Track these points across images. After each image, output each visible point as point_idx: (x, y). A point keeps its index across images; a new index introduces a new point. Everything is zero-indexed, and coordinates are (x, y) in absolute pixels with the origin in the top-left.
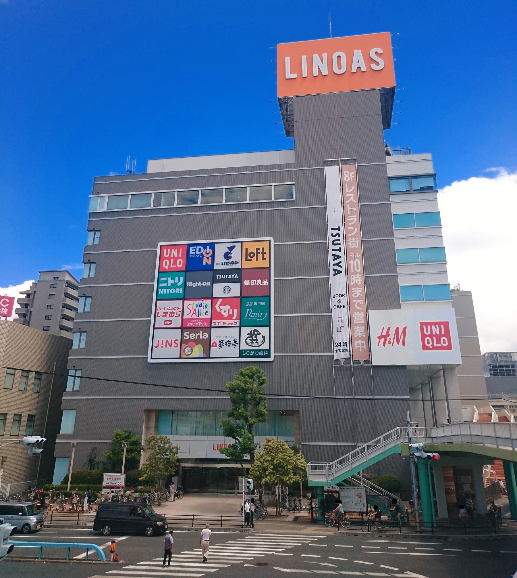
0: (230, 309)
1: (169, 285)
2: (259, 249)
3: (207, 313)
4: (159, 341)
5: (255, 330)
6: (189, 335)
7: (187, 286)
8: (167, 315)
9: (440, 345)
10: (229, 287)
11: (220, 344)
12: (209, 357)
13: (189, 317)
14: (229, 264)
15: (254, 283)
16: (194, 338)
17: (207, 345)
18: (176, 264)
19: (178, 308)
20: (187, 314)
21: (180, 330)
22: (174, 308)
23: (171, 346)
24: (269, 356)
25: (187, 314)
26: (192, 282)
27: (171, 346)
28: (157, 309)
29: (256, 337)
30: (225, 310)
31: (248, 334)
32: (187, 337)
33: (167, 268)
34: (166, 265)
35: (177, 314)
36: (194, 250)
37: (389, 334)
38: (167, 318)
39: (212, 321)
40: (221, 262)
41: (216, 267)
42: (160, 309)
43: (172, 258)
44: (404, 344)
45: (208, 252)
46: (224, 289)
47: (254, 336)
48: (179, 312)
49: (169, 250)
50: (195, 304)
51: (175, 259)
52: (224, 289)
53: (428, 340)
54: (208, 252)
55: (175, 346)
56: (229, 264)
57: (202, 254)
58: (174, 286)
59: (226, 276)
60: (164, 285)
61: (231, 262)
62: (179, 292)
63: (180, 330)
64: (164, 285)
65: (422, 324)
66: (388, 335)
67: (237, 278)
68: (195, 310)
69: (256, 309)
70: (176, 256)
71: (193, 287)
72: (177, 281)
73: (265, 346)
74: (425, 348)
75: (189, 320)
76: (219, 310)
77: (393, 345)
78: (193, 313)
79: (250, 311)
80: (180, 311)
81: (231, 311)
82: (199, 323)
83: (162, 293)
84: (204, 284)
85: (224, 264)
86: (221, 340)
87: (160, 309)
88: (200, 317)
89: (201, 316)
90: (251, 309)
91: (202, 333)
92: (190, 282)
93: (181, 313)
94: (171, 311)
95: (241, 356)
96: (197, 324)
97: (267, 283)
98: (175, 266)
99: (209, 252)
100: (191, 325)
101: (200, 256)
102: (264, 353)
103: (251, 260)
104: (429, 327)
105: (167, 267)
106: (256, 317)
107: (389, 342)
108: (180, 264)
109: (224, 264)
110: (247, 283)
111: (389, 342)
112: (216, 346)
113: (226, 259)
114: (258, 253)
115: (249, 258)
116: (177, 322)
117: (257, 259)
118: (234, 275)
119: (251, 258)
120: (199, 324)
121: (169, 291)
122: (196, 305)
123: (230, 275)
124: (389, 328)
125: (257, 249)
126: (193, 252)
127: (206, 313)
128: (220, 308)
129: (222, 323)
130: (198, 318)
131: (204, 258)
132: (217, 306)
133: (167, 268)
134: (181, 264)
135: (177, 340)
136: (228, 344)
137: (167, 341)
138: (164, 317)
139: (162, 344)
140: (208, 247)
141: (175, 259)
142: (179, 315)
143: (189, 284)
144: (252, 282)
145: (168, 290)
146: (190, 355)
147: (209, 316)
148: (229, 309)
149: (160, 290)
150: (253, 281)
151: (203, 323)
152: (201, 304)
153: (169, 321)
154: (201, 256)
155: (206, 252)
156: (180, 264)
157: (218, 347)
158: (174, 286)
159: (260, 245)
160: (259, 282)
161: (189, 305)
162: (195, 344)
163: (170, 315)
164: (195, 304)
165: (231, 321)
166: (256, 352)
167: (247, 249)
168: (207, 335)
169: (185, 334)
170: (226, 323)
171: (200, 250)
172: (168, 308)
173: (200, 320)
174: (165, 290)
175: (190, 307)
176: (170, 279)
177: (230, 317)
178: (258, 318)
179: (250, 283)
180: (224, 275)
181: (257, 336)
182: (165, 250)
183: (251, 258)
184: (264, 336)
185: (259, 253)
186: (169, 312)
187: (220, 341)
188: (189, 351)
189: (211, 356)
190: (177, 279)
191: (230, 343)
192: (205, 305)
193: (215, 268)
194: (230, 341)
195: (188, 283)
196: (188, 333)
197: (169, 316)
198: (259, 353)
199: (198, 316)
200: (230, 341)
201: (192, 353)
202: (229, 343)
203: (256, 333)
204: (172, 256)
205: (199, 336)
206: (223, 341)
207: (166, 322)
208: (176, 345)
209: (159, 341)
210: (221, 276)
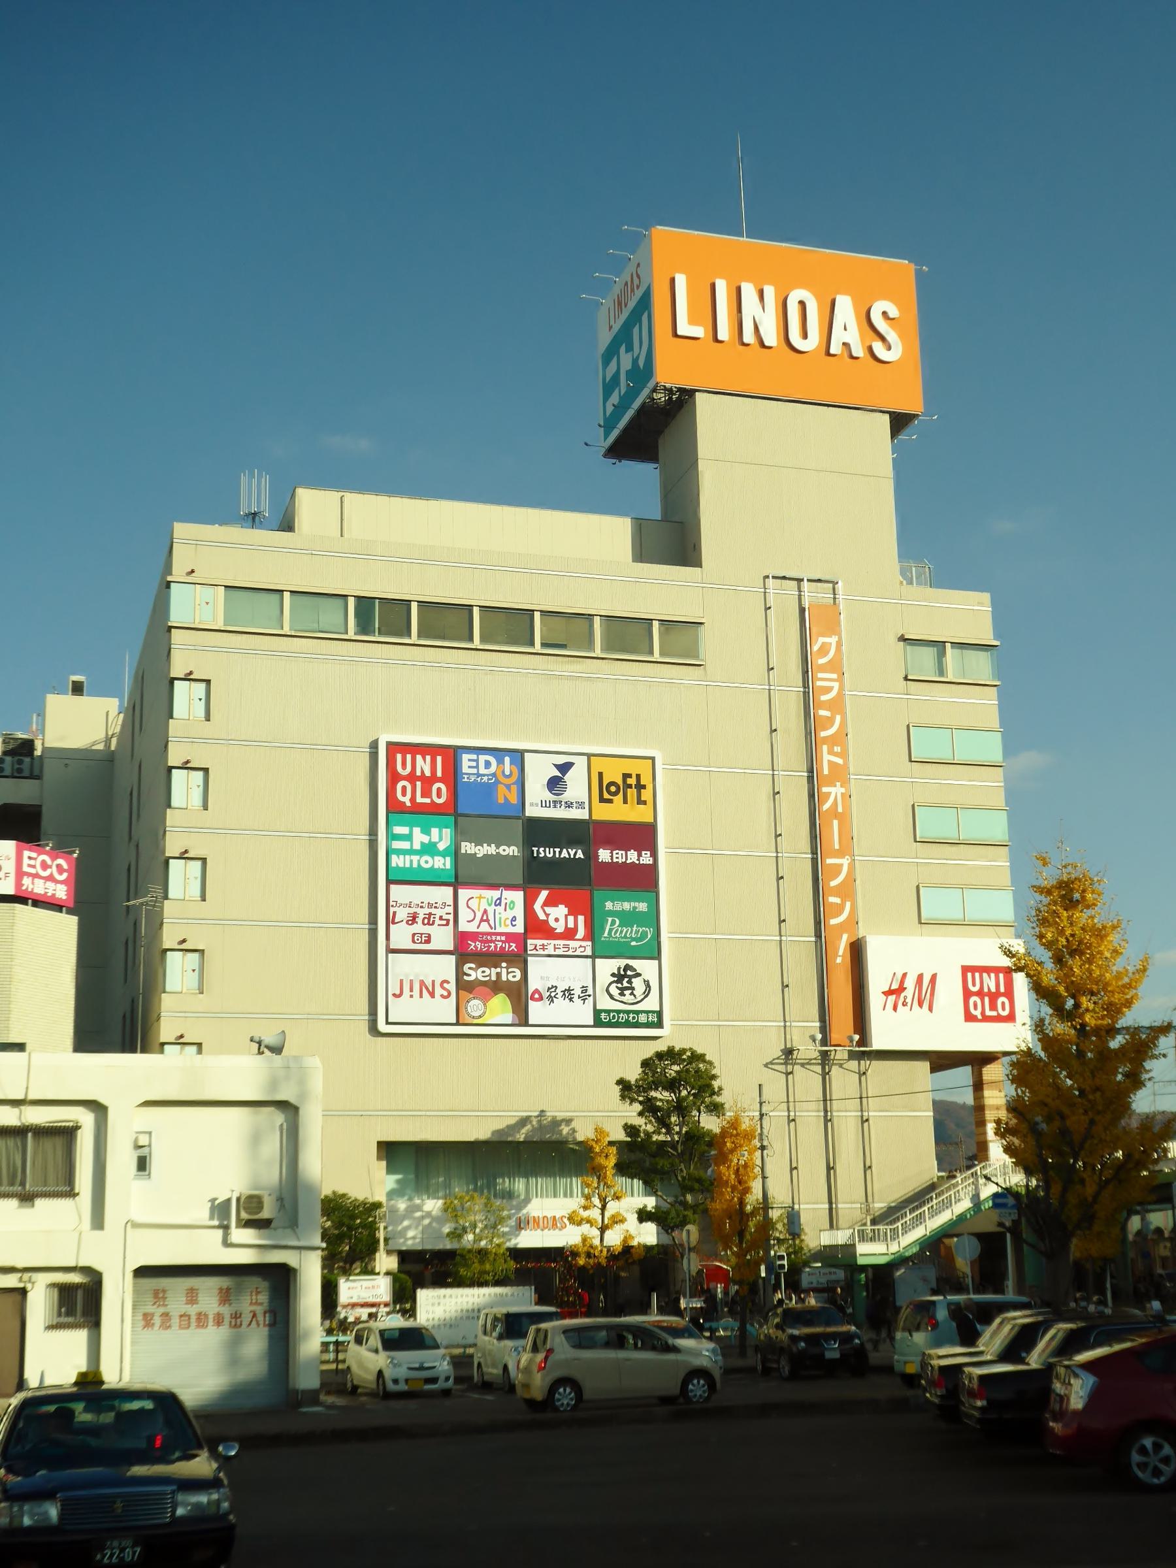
0: (570, 914)
1: (417, 846)
2: (630, 776)
3: (515, 921)
5: (627, 967)
7: (463, 851)
11: (550, 995)
12: (525, 1023)
13: (472, 928)
14: (560, 807)
15: (620, 857)
16: (488, 978)
17: (519, 997)
19: (444, 904)
20: (468, 921)
21: (453, 958)
22: (434, 905)
23: (432, 995)
24: (659, 1024)
25: (468, 921)
26: (473, 844)
27: (432, 995)
28: (391, 903)
29: (630, 982)
31: (613, 975)
32: (469, 975)
33: (408, 804)
34: (404, 794)
35: (441, 918)
36: (474, 764)
37: (905, 986)
38: (419, 928)
39: (530, 942)
40: (542, 801)
42: (398, 905)
43: (419, 778)
44: (931, 1009)
45: (507, 772)
47: (626, 980)
48: (447, 914)
49: (409, 757)
50: (485, 898)
51: (428, 782)
54: (507, 772)
55: (442, 996)
56: (560, 807)
57: (494, 775)
58: (429, 849)
60: (405, 845)
61: (566, 803)
62: (442, 867)
63: (453, 958)
64: (405, 845)
65: (966, 970)
66: (902, 989)
68: (485, 912)
69: (628, 919)
71: (478, 856)
72: (435, 838)
73: (651, 1004)
74: (969, 1018)
75: (474, 936)
76: (542, 917)
78: (482, 920)
79: (613, 923)
80: (450, 914)
81: (571, 919)
82: (497, 943)
83: (401, 865)
85: (550, 807)
86: (553, 987)
87: (398, 905)
88: (499, 930)
89: (501, 926)
90: (616, 919)
91: (507, 968)
93: (451, 917)
94: (427, 911)
95: (598, 1023)
96: (493, 945)
97: (651, 859)
98: (428, 801)
100: (479, 946)
101: (489, 779)
102: (648, 1018)
103: (610, 801)
104: (977, 975)
105: (406, 800)
107: (904, 1004)
108: (439, 795)
109: (550, 807)
111: (904, 1004)
113: (552, 793)
115: (606, 796)
116: (443, 938)
117: (625, 802)
119: (612, 797)
120: (498, 945)
121: (419, 861)
122: (488, 899)
124: (905, 975)
125: (626, 776)
126: (469, 767)
127: (512, 920)
128: (544, 911)
129: (551, 945)
130: (493, 931)
132: (537, 906)
133: (408, 804)
134: (440, 794)
135: (448, 982)
136: (567, 995)
137: (422, 983)
138: (410, 925)
139: (411, 990)
140: (507, 760)
142: (448, 921)
143: (467, 848)
144: (617, 856)
145: (415, 858)
146: (480, 1017)
147: (520, 928)
148: (566, 916)
149: (394, 858)
150: (617, 854)
152: (500, 899)
153: (423, 936)
154: (492, 779)
155: (503, 772)
156: (439, 795)
158: (429, 849)
159: (633, 768)
160: (632, 856)
161: (470, 899)
163: (426, 921)
164: (485, 898)
165: (572, 944)
167: (600, 775)
168: (518, 974)
170: (561, 947)
171: (488, 764)
172: (419, 903)
173: (498, 938)
174: (407, 857)
176: (417, 831)
177: (569, 934)
179: (612, 856)
181: (633, 980)
183: (612, 797)
184: (648, 981)
185: (630, 786)
186: (422, 913)
187: (549, 989)
189: (530, 1023)
190: (435, 832)
191: (572, 992)
193: (528, 814)
194: (573, 990)
195: (463, 844)
196: (473, 965)
197: (423, 924)
198: (638, 1017)
199: (493, 927)
200: (573, 990)
202: (570, 994)
203: (629, 973)
205: (499, 975)
206: (556, 987)
207: (416, 938)
208: (445, 993)
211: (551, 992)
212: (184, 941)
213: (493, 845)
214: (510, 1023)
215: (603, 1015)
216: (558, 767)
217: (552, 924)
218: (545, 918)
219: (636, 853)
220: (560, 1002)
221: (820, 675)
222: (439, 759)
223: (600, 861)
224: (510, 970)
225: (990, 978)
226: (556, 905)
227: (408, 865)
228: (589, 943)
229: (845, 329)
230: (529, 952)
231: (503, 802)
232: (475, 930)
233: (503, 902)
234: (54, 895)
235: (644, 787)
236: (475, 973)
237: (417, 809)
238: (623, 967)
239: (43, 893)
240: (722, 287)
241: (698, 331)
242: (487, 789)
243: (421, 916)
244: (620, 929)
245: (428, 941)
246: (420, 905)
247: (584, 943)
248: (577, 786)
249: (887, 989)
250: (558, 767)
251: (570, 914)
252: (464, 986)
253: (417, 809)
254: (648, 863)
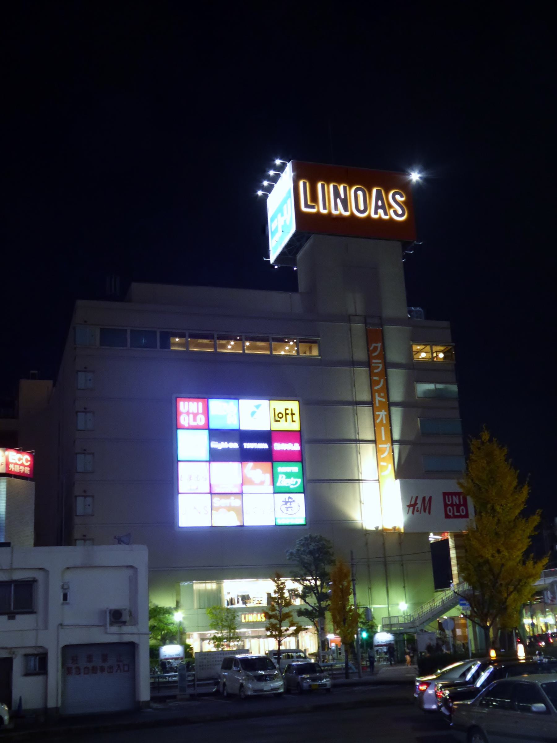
5: (290, 498)
9: (458, 514)
31: (283, 501)
44: (429, 513)
51: (195, 415)
53: (450, 509)
65: (445, 494)
66: (416, 504)
74: (447, 516)
103: (279, 421)
104: (450, 496)
114: (286, 414)
124: (417, 498)
125: (286, 409)
141: (195, 415)
177: (262, 483)
181: (292, 503)
185: (288, 414)
221: (374, 361)
225: (456, 498)
234: (24, 472)
235: (294, 414)
239: (18, 471)
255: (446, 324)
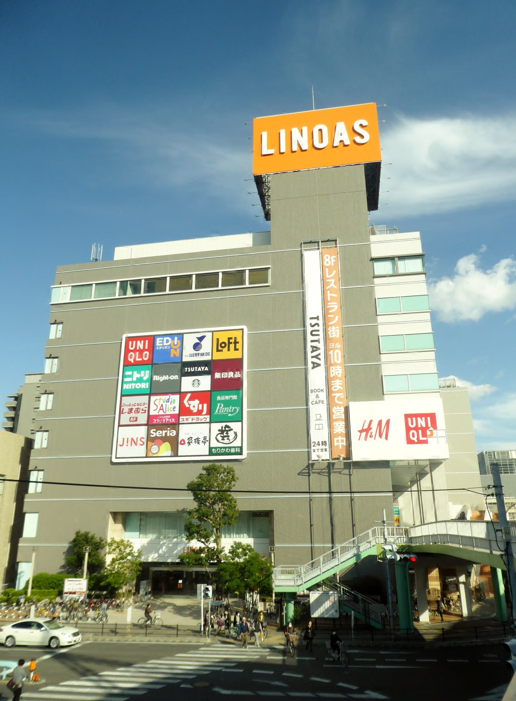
0: (200, 403)
1: (135, 379)
2: (231, 338)
4: (124, 439)
5: (227, 426)
6: (156, 432)
7: (154, 380)
8: (132, 411)
10: (199, 381)
11: (189, 442)
12: (177, 456)
13: (155, 413)
15: (225, 376)
16: (161, 435)
18: (142, 358)
19: (144, 404)
24: (241, 453)
26: (159, 376)
27: (136, 444)
28: (122, 405)
29: (227, 433)
30: (195, 405)
31: (219, 430)
32: (153, 435)
33: (133, 362)
35: (142, 410)
36: (162, 342)
37: (371, 427)
38: (133, 415)
39: (181, 417)
41: (185, 359)
44: (386, 438)
45: (176, 343)
46: (193, 382)
47: (225, 432)
48: (145, 408)
49: (134, 342)
51: (141, 352)
52: (193, 382)
53: (413, 434)
54: (176, 343)
55: (141, 445)
57: (170, 345)
58: (140, 380)
59: (195, 369)
60: (129, 379)
61: (201, 354)
62: (145, 387)
64: (129, 379)
65: (407, 416)
66: (369, 428)
67: (207, 370)
68: (162, 405)
69: (227, 403)
70: (142, 348)
71: (160, 381)
74: (410, 441)
75: (156, 417)
76: (187, 405)
77: (375, 439)
78: (160, 409)
79: (220, 406)
81: (200, 406)
83: (127, 388)
84: (172, 377)
86: (190, 438)
88: (167, 413)
92: (156, 376)
93: (147, 409)
94: (137, 407)
95: (211, 454)
98: (141, 359)
99: (177, 343)
100: (158, 421)
101: (167, 347)
102: (235, 450)
103: (221, 351)
104: (414, 419)
105: (132, 360)
106: (227, 411)
110: (217, 375)
111: (371, 436)
112: (184, 444)
114: (230, 343)
115: (220, 348)
116: (143, 418)
117: (229, 350)
118: (204, 367)
120: (167, 419)
121: (135, 386)
123: (200, 368)
124: (371, 422)
125: (229, 339)
126: (160, 343)
127: (174, 408)
129: (190, 418)
130: (165, 414)
131: (172, 349)
132: (185, 401)
133: (133, 362)
135: (143, 438)
137: (132, 439)
138: (130, 413)
139: (127, 443)
140: (176, 338)
142: (145, 411)
143: (156, 378)
144: (224, 375)
145: (133, 385)
146: (157, 453)
147: (177, 412)
148: (198, 404)
150: (224, 374)
151: (171, 419)
152: (169, 399)
154: (169, 347)
155: (174, 343)
157: (187, 444)
158: (140, 380)
160: (231, 375)
161: (155, 400)
162: (162, 442)
163: (136, 412)
166: (227, 449)
167: (218, 339)
169: (152, 432)
171: (167, 341)
173: (167, 417)
174: (130, 384)
175: (156, 402)
177: (199, 413)
178: (229, 413)
179: (221, 376)
180: (194, 368)
181: (229, 432)
182: (130, 342)
184: (236, 432)
185: (231, 343)
186: (134, 408)
187: (188, 439)
188: (156, 449)
191: (199, 440)
192: (172, 400)
193: (183, 361)
195: (154, 376)
196: (155, 430)
201: (159, 451)
202: (198, 441)
203: (227, 429)
204: (138, 348)
205: (166, 433)
206: (192, 438)
207: (131, 419)
208: (142, 443)
209: (124, 439)
210: (190, 369)
211: (189, 440)
212: (41, 428)
213: (167, 376)
214: (170, 455)
215: (213, 450)
216: (198, 338)
217: (192, 408)
218: (188, 406)
219: (233, 373)
220: (193, 444)
222: (147, 341)
223: (215, 378)
224: (171, 431)
225: (422, 420)
226: (194, 400)
227: (130, 388)
228: (209, 416)
229: (341, 135)
230: (180, 422)
231: (173, 356)
232: (157, 414)
233: (170, 400)
235: (238, 343)
236: (154, 433)
237: (136, 364)
238: (224, 426)
240: (283, 132)
241: (272, 151)
242: (166, 352)
243: (134, 410)
244: (223, 408)
245: (136, 421)
246: (134, 405)
247: (206, 416)
248: (207, 346)
249: (361, 429)
250: (198, 338)
251: (200, 403)
252: (150, 439)
253: (136, 364)
254: (238, 377)
255: (417, 234)
